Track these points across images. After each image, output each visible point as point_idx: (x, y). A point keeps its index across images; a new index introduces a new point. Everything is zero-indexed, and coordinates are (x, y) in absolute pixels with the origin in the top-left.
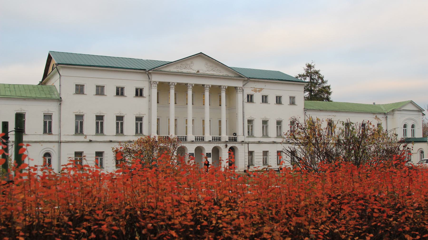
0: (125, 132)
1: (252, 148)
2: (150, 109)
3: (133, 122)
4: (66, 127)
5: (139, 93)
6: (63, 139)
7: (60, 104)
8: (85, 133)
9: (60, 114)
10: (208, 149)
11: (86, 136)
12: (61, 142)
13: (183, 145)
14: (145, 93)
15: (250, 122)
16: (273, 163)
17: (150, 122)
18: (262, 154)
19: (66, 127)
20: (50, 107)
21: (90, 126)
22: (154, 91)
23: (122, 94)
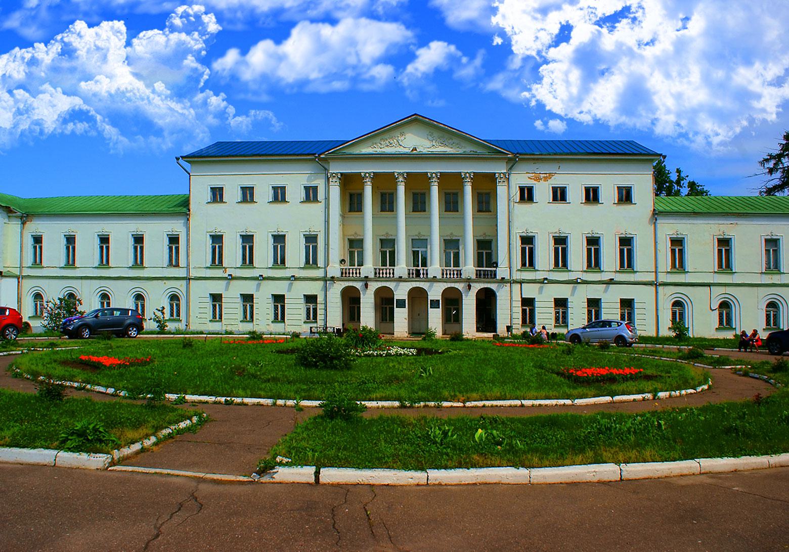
0: (256, 263)
1: (530, 291)
2: (327, 222)
3: (517, 245)
4: (198, 253)
5: (311, 194)
6: (193, 274)
7: (188, 220)
8: (224, 266)
9: (188, 235)
10: (435, 292)
11: (225, 268)
12: (189, 279)
13: (388, 284)
14: (321, 195)
15: (528, 240)
16: (264, 322)
17: (327, 245)
18: (553, 304)
19: (198, 253)
20: (176, 226)
21: (232, 252)
22: (335, 191)
23: (284, 200)
